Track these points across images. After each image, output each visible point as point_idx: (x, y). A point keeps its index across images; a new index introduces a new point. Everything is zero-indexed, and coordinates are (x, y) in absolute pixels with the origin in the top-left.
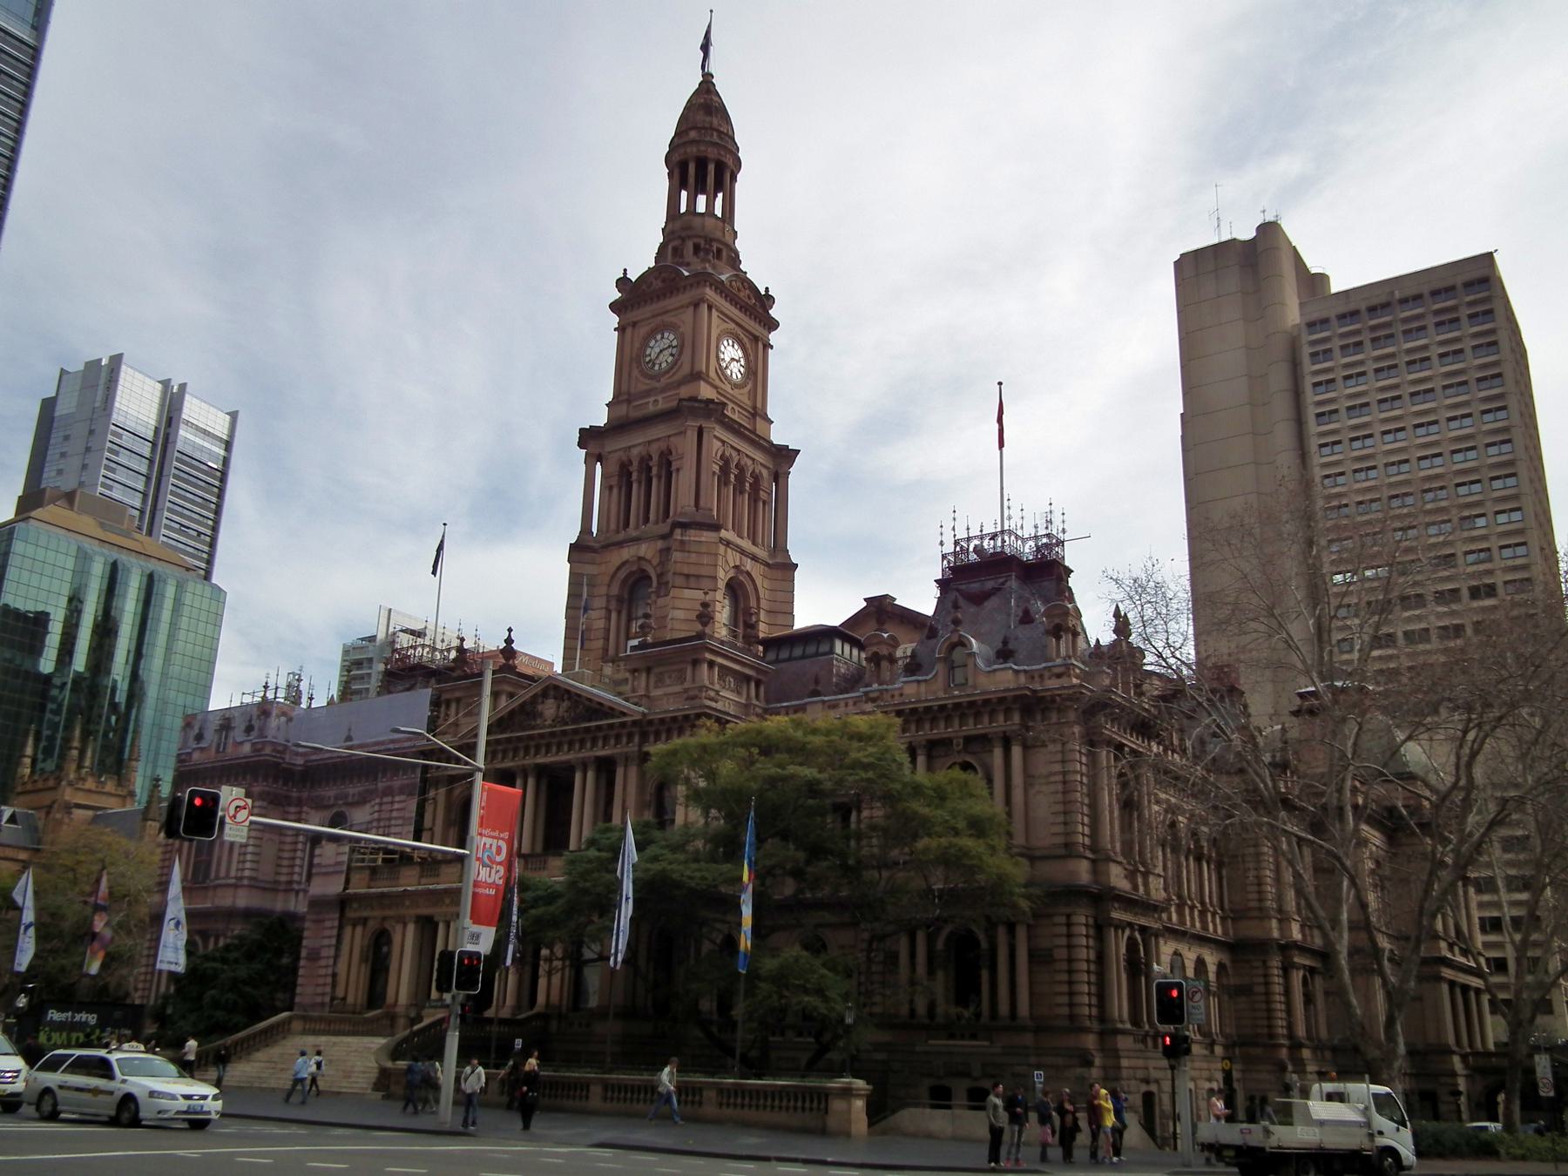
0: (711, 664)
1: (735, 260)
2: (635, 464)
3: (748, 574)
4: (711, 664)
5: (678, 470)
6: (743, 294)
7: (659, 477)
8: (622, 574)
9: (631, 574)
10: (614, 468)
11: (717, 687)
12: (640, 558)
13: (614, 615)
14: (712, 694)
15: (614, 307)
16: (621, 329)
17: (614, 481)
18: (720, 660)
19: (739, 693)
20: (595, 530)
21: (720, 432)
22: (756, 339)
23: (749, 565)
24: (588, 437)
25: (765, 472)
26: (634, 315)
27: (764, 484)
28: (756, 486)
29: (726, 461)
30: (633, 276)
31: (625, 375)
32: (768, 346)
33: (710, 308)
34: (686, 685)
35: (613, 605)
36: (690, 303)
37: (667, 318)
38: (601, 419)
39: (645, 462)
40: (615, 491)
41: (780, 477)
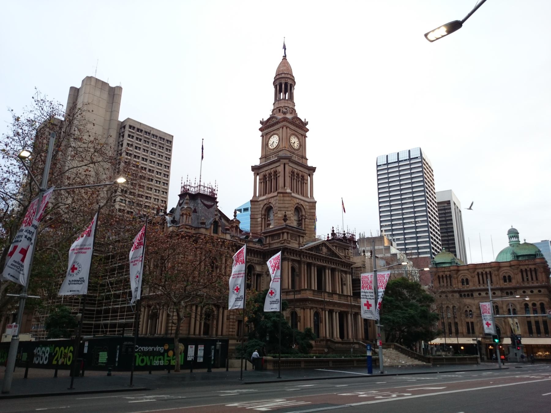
0: (288, 233)
1: (293, 111)
2: (267, 175)
3: (301, 205)
5: (279, 176)
6: (297, 122)
7: (274, 179)
8: (265, 208)
9: (267, 207)
10: (262, 177)
11: (289, 239)
12: (270, 203)
13: (263, 219)
14: (288, 242)
15: (261, 130)
16: (262, 136)
17: (262, 181)
18: (290, 232)
19: (296, 241)
20: (257, 195)
21: (291, 164)
22: (302, 135)
23: (302, 203)
24: (255, 169)
26: (266, 131)
27: (305, 178)
29: (293, 172)
31: (264, 150)
32: (305, 137)
33: (287, 128)
34: (281, 239)
35: (263, 217)
36: (281, 127)
37: (275, 132)
38: (257, 163)
39: (270, 174)
40: (263, 183)
41: (311, 175)
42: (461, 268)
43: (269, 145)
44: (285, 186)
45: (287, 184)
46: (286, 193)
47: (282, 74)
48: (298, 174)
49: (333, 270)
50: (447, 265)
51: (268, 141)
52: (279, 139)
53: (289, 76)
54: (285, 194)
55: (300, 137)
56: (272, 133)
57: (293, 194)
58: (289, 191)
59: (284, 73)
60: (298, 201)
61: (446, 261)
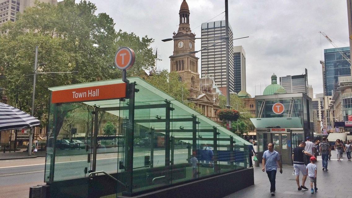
0: (193, 92)
4: (193, 92)
18: (194, 91)
21: (191, 58)
23: (194, 75)
25: (195, 61)
28: (194, 64)
29: (190, 61)
30: (177, 32)
38: (172, 54)
42: (250, 100)
43: (178, 46)
44: (188, 68)
45: (189, 68)
46: (189, 72)
47: (184, 9)
48: (192, 62)
49: (207, 106)
50: (244, 98)
51: (178, 44)
52: (184, 44)
53: (187, 11)
54: (188, 73)
55: (192, 42)
56: (180, 40)
57: (192, 72)
58: (190, 71)
59: (186, 9)
60: (192, 75)
61: (244, 96)
